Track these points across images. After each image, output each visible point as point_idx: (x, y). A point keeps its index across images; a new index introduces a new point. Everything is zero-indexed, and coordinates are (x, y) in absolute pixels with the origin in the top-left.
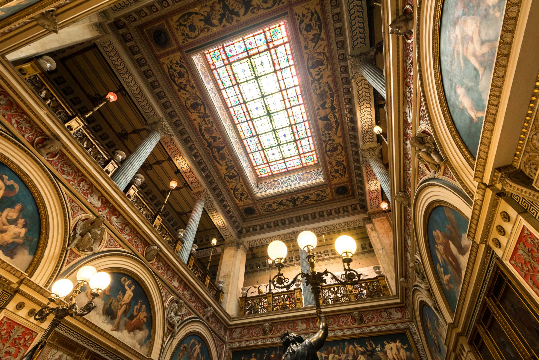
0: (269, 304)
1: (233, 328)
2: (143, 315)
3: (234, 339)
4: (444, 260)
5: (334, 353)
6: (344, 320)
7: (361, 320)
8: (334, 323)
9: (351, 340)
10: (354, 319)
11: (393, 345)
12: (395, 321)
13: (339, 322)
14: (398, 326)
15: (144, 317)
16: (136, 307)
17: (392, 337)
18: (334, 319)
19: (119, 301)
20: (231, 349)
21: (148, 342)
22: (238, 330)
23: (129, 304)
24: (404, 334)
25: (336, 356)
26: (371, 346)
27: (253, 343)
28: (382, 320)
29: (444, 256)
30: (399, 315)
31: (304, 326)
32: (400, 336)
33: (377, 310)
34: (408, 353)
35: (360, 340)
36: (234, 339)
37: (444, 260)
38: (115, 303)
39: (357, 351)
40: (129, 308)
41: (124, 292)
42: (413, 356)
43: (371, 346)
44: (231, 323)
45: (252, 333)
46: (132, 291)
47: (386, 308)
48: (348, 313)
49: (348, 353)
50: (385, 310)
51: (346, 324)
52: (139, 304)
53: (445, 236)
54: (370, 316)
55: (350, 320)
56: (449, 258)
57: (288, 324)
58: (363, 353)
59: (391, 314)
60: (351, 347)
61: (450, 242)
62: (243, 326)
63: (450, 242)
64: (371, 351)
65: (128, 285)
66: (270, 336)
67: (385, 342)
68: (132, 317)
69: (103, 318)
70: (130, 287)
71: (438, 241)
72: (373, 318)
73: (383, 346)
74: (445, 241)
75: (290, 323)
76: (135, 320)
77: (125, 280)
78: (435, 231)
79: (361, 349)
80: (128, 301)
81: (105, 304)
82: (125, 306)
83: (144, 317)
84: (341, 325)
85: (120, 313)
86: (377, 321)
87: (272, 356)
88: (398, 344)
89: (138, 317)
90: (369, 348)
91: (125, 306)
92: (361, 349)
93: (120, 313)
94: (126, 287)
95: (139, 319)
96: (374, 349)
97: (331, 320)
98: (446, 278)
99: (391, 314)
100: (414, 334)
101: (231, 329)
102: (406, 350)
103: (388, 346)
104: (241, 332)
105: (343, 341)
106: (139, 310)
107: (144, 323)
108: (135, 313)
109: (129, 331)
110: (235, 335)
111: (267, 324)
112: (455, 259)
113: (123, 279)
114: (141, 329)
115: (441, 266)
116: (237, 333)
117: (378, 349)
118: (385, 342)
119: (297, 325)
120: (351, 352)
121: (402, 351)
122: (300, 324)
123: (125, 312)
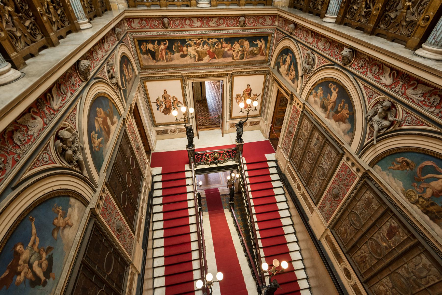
2: (345, 112)
4: (101, 128)
15: (347, 114)
16: (340, 105)
19: (328, 100)
21: (350, 134)
23: (335, 103)
29: (101, 126)
37: (101, 128)
38: (326, 101)
40: (335, 106)
41: (331, 93)
46: (337, 93)
52: (343, 103)
53: (105, 113)
56: (105, 127)
61: (108, 118)
63: (108, 118)
65: (333, 89)
68: (337, 112)
69: (321, 109)
70: (335, 89)
71: (99, 115)
74: (105, 116)
76: (339, 114)
77: (331, 85)
78: (99, 108)
80: (334, 100)
81: (321, 102)
82: (332, 103)
83: (347, 114)
85: (329, 108)
89: (342, 112)
91: (332, 103)
93: (329, 108)
94: (332, 90)
95: (342, 114)
98: (97, 141)
106: (342, 108)
107: (347, 118)
108: (339, 110)
109: (336, 121)
112: (108, 127)
113: (330, 84)
114: (344, 122)
115: (96, 133)
123: (333, 108)
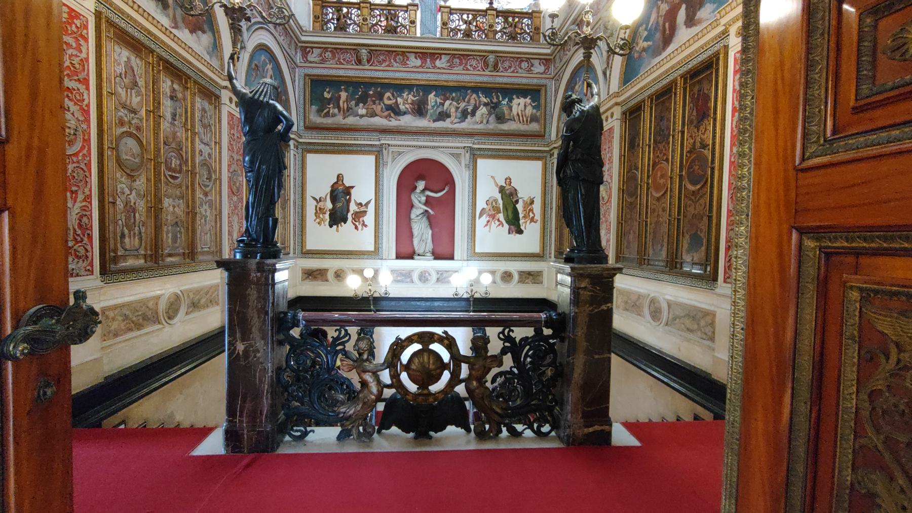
0: (365, 20)
1: (307, 47)
3: (311, 62)
5: (453, 99)
6: (474, 63)
7: (495, 67)
8: (460, 64)
9: (476, 89)
10: (486, 65)
11: (522, 101)
12: (535, 75)
13: (466, 64)
14: (535, 81)
17: (523, 92)
18: (461, 60)
20: (308, 75)
22: (317, 52)
24: (539, 91)
25: (454, 103)
26: (498, 98)
27: (341, 73)
28: (520, 71)
30: (541, 69)
31: (418, 62)
32: (534, 93)
33: (518, 58)
34: (535, 111)
35: (487, 90)
36: (311, 62)
39: (480, 102)
42: (538, 114)
43: (498, 98)
44: (303, 38)
45: (339, 59)
47: (529, 59)
48: (483, 56)
49: (468, 102)
50: (528, 60)
51: (474, 68)
54: (507, 64)
55: (481, 65)
57: (395, 56)
58: (486, 105)
59: (532, 65)
60: (474, 95)
62: (325, 48)
64: (496, 103)
66: (367, 67)
67: (514, 97)
72: (510, 67)
73: (511, 100)
75: (398, 55)
79: (485, 100)
84: (468, 69)
86: (513, 72)
87: (371, 92)
88: (528, 100)
90: (495, 100)
92: (485, 100)
96: (500, 102)
97: (458, 61)
99: (532, 65)
100: (549, 93)
101: (305, 50)
102: (534, 107)
103: (516, 101)
104: (321, 55)
105: (466, 88)
110: (311, 58)
111: (364, 51)
116: (314, 55)
117: (504, 102)
118: (514, 97)
119: (408, 59)
120: (472, 102)
121: (529, 108)
122: (412, 57)
